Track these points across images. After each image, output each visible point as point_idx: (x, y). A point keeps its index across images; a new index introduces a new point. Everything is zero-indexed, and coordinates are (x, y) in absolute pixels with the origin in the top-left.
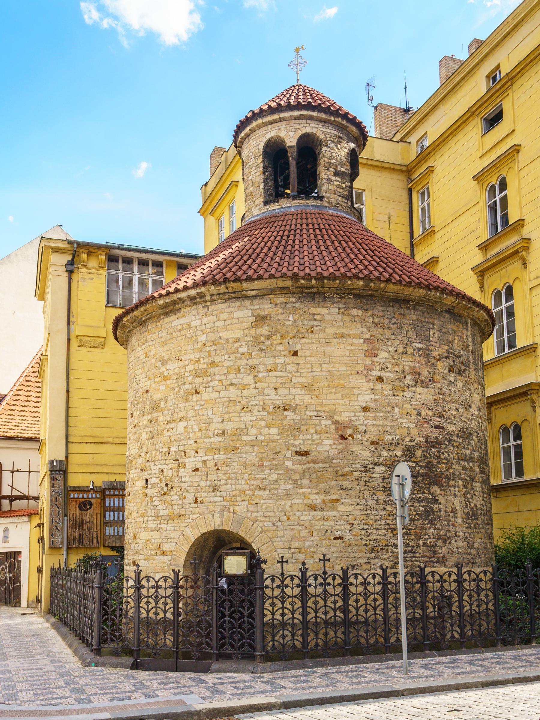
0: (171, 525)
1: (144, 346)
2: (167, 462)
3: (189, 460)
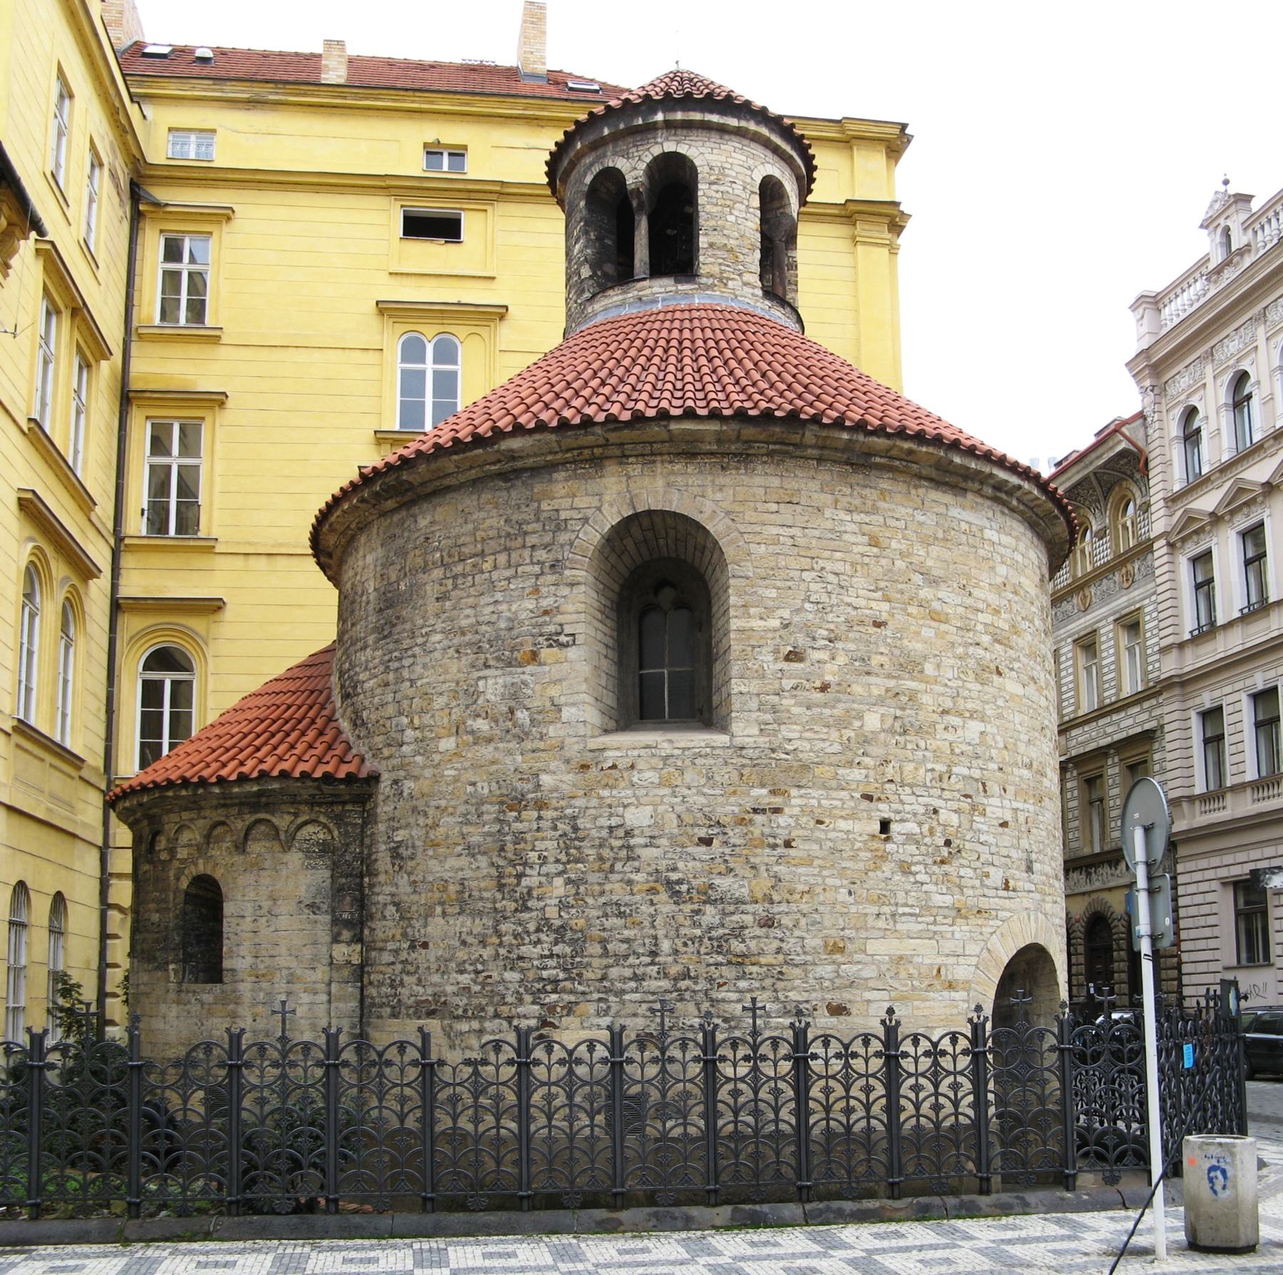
0: (961, 930)
2: (947, 794)
3: (992, 801)
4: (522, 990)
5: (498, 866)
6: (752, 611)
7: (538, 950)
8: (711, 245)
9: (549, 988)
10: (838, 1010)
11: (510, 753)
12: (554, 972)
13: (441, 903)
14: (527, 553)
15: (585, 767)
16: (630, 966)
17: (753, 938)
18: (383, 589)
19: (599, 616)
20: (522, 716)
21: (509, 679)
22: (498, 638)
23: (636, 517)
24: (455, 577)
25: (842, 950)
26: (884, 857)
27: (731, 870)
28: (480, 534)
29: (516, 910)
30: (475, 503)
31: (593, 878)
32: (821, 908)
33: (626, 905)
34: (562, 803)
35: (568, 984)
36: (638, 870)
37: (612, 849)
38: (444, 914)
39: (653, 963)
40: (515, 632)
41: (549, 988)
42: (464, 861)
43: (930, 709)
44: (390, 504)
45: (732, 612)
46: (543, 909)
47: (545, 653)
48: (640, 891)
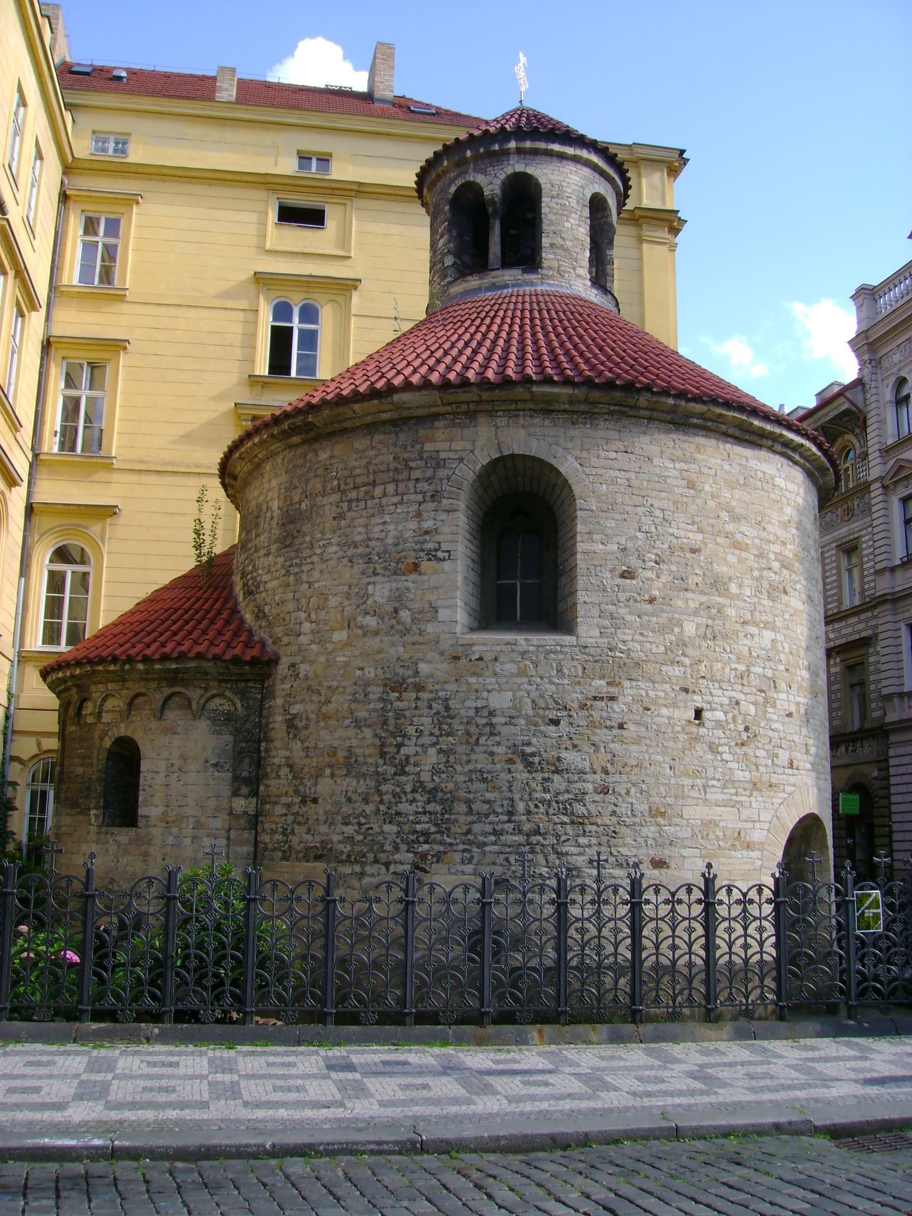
0: (757, 801)
1: (683, 466)
2: (746, 690)
4: (398, 840)
5: (381, 738)
6: (595, 537)
7: (413, 808)
8: (552, 245)
9: (421, 839)
10: (659, 864)
11: (393, 644)
12: (427, 826)
13: (330, 766)
14: (411, 484)
15: (456, 658)
16: (490, 823)
17: (594, 801)
18: (285, 509)
19: (468, 536)
20: (405, 615)
21: (394, 585)
22: (385, 551)
23: (502, 458)
24: (350, 501)
25: (663, 815)
26: (697, 739)
27: (575, 746)
28: (371, 468)
29: (395, 774)
30: (368, 442)
31: (461, 749)
32: (647, 779)
33: (488, 772)
34: (437, 687)
35: (438, 837)
36: (499, 744)
37: (477, 726)
38: (333, 775)
39: (509, 821)
40: (400, 548)
41: (421, 839)
42: (351, 732)
43: (734, 620)
44: (295, 439)
45: (579, 538)
46: (418, 774)
47: (425, 566)
48: (500, 761)
